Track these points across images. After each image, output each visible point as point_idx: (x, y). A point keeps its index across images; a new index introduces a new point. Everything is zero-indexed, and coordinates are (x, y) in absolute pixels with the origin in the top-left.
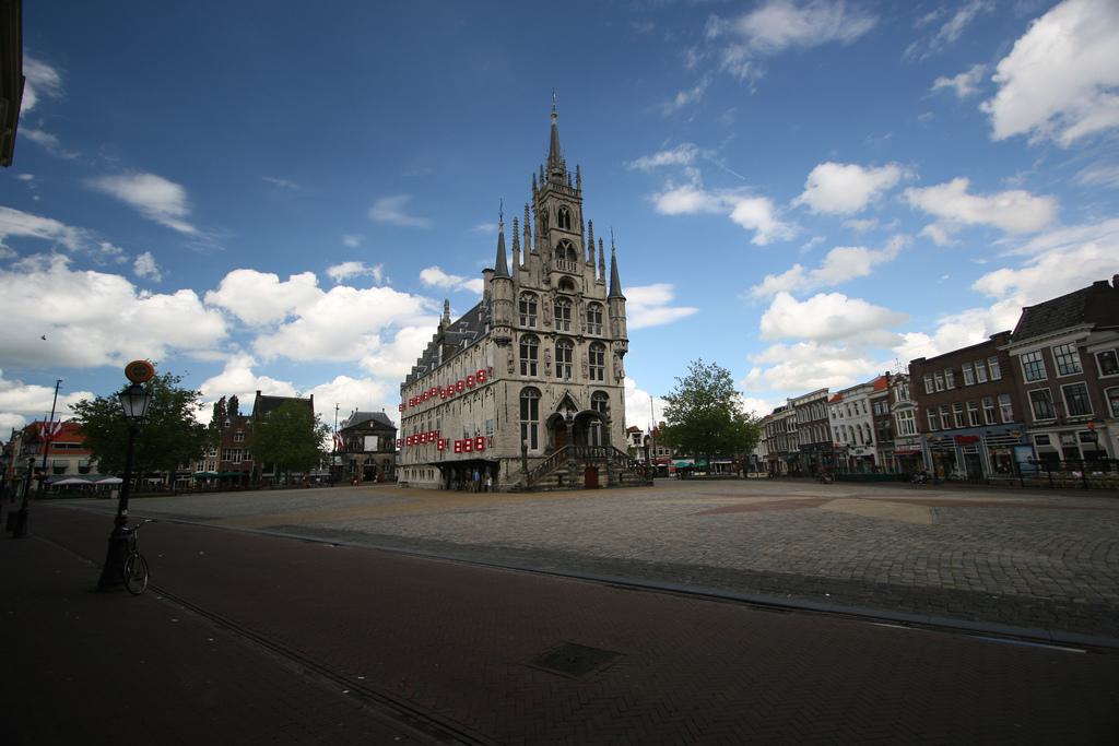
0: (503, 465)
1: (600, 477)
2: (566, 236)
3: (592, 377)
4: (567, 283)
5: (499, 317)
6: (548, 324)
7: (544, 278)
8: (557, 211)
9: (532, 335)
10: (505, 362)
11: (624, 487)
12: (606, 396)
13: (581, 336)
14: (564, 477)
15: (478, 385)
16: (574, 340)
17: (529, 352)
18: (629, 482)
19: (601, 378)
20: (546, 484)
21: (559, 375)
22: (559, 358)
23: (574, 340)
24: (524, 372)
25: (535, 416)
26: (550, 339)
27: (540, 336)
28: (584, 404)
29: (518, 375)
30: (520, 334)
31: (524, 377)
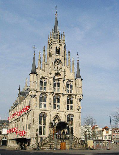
0: (32, 140)
1: (66, 146)
2: (58, 57)
8: (55, 49)
11: (76, 150)
12: (74, 116)
13: (64, 94)
14: (52, 145)
15: (27, 110)
16: (61, 95)
17: (43, 99)
18: (78, 148)
19: (71, 109)
20: (45, 147)
21: (55, 108)
22: (55, 101)
23: (61, 95)
25: (45, 123)
28: (64, 119)
30: (40, 93)
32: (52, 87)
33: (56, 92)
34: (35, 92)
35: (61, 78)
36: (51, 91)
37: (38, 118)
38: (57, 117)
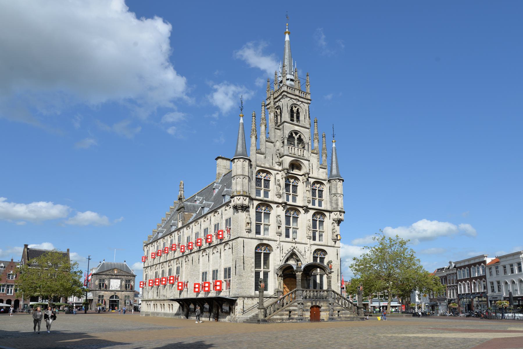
3: (314, 239)
4: (295, 165)
5: (239, 188)
6: (280, 196)
7: (277, 160)
9: (266, 204)
10: (244, 224)
16: (301, 209)
21: (287, 236)
22: (288, 222)
23: (301, 209)
24: (258, 232)
26: (281, 208)
27: (271, 204)
28: (307, 259)
29: (253, 234)
30: (256, 203)
31: (258, 236)
32: (283, 191)
33: (290, 202)
34: (248, 198)
35: (301, 174)
36: (280, 201)
37: (254, 256)
38: (293, 255)
